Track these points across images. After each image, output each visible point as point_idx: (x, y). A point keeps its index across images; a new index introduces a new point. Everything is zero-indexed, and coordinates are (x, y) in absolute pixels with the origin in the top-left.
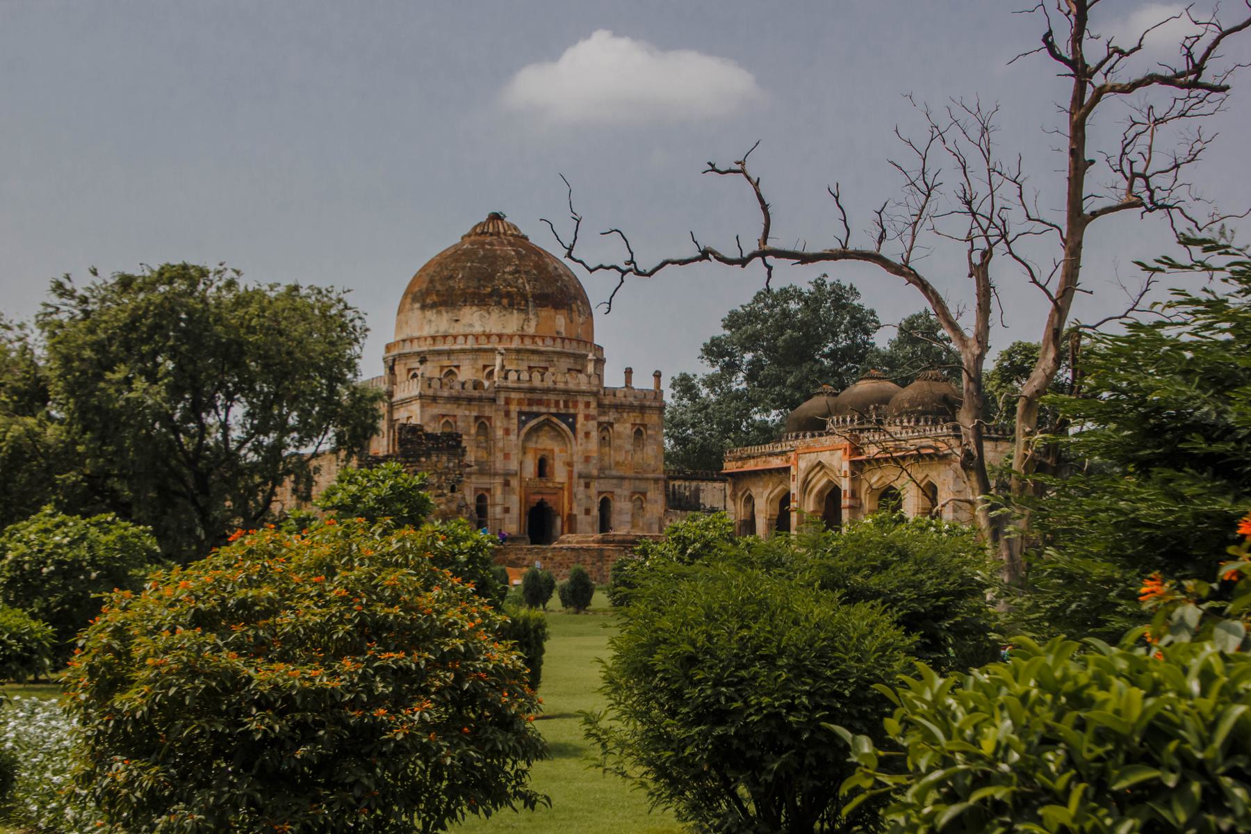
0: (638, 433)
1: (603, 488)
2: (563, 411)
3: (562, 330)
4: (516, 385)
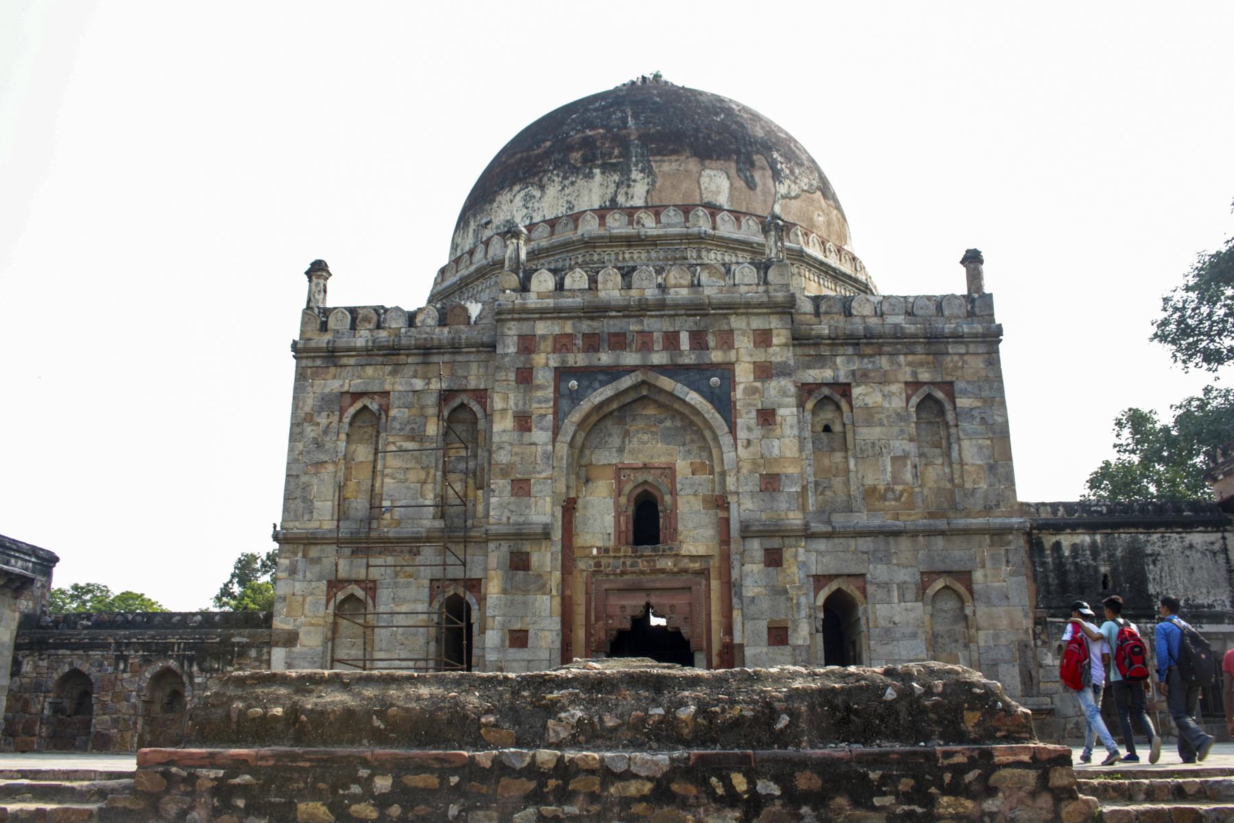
0: (933, 407)
1: (828, 565)
2: (689, 359)
3: (723, 200)
4: (550, 302)
